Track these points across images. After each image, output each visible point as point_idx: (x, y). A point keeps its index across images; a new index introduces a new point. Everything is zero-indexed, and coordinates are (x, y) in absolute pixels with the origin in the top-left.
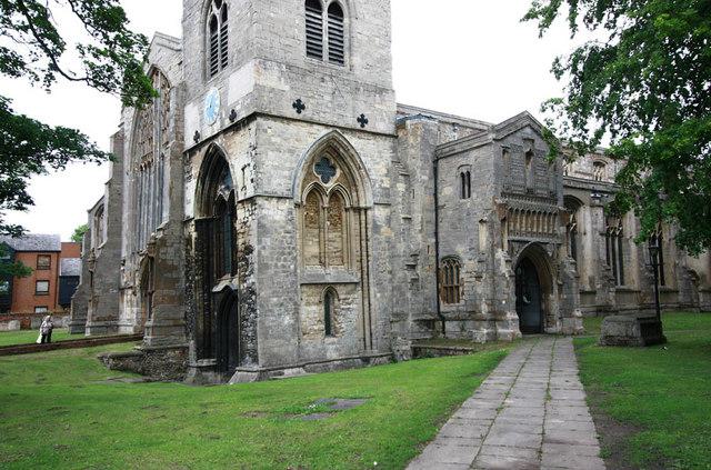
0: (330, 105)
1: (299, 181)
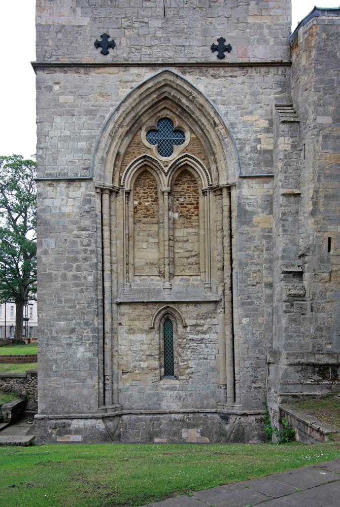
0: (159, 34)
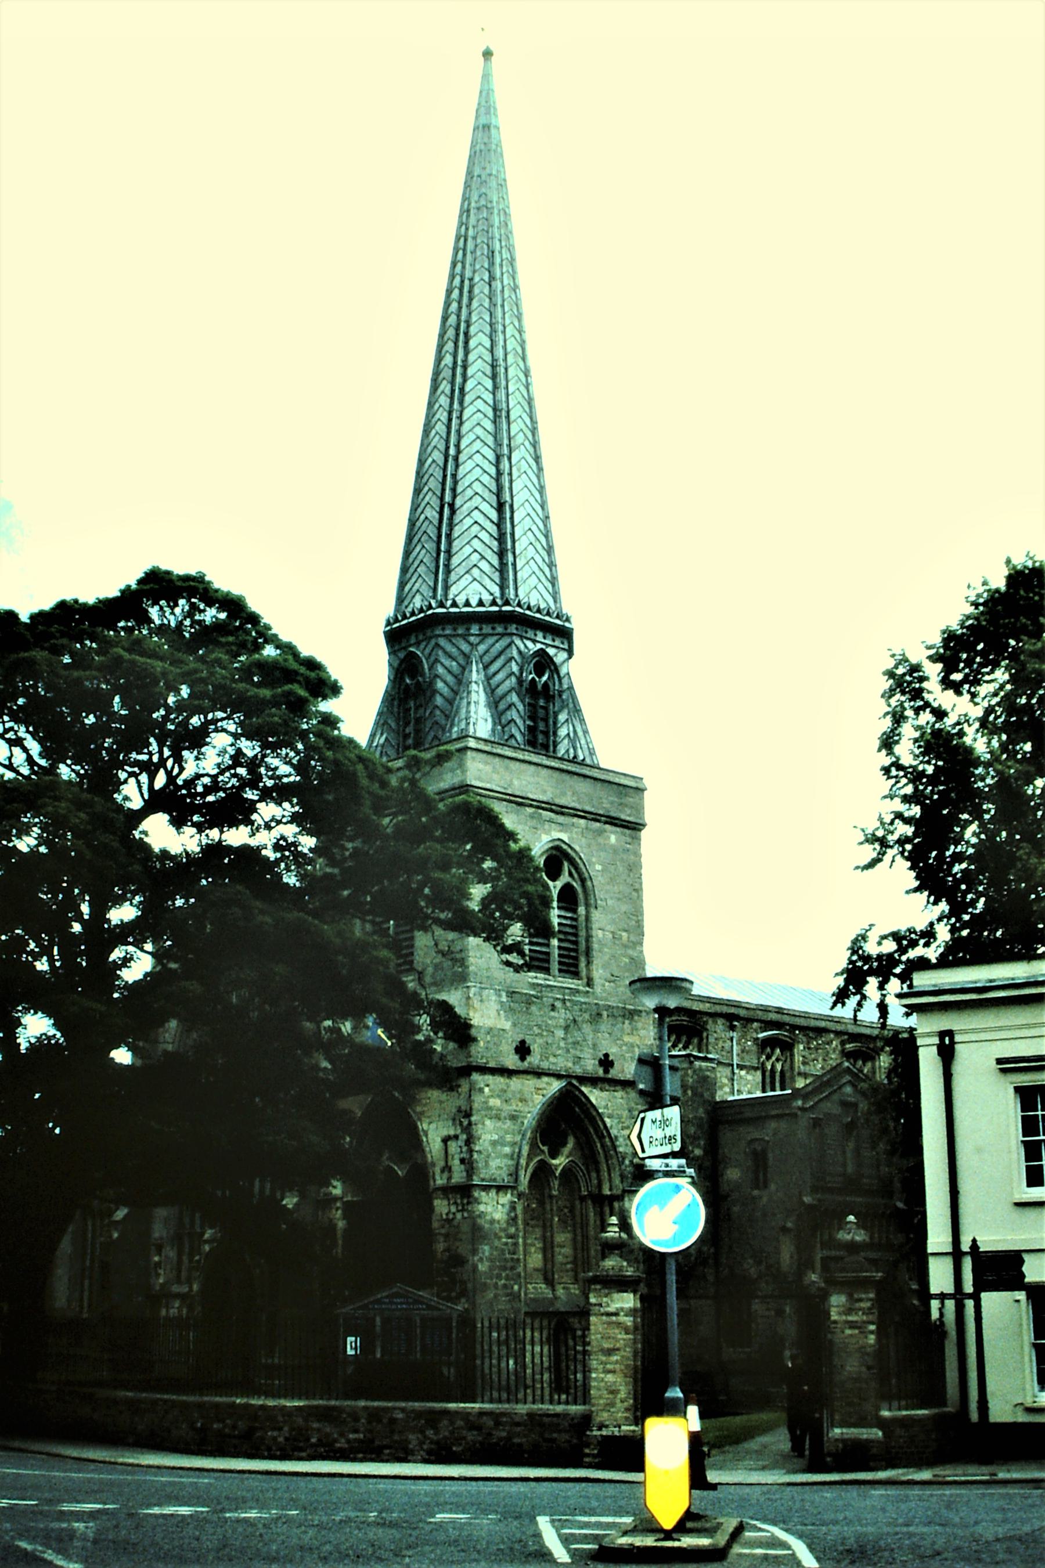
1: (523, 1162)
